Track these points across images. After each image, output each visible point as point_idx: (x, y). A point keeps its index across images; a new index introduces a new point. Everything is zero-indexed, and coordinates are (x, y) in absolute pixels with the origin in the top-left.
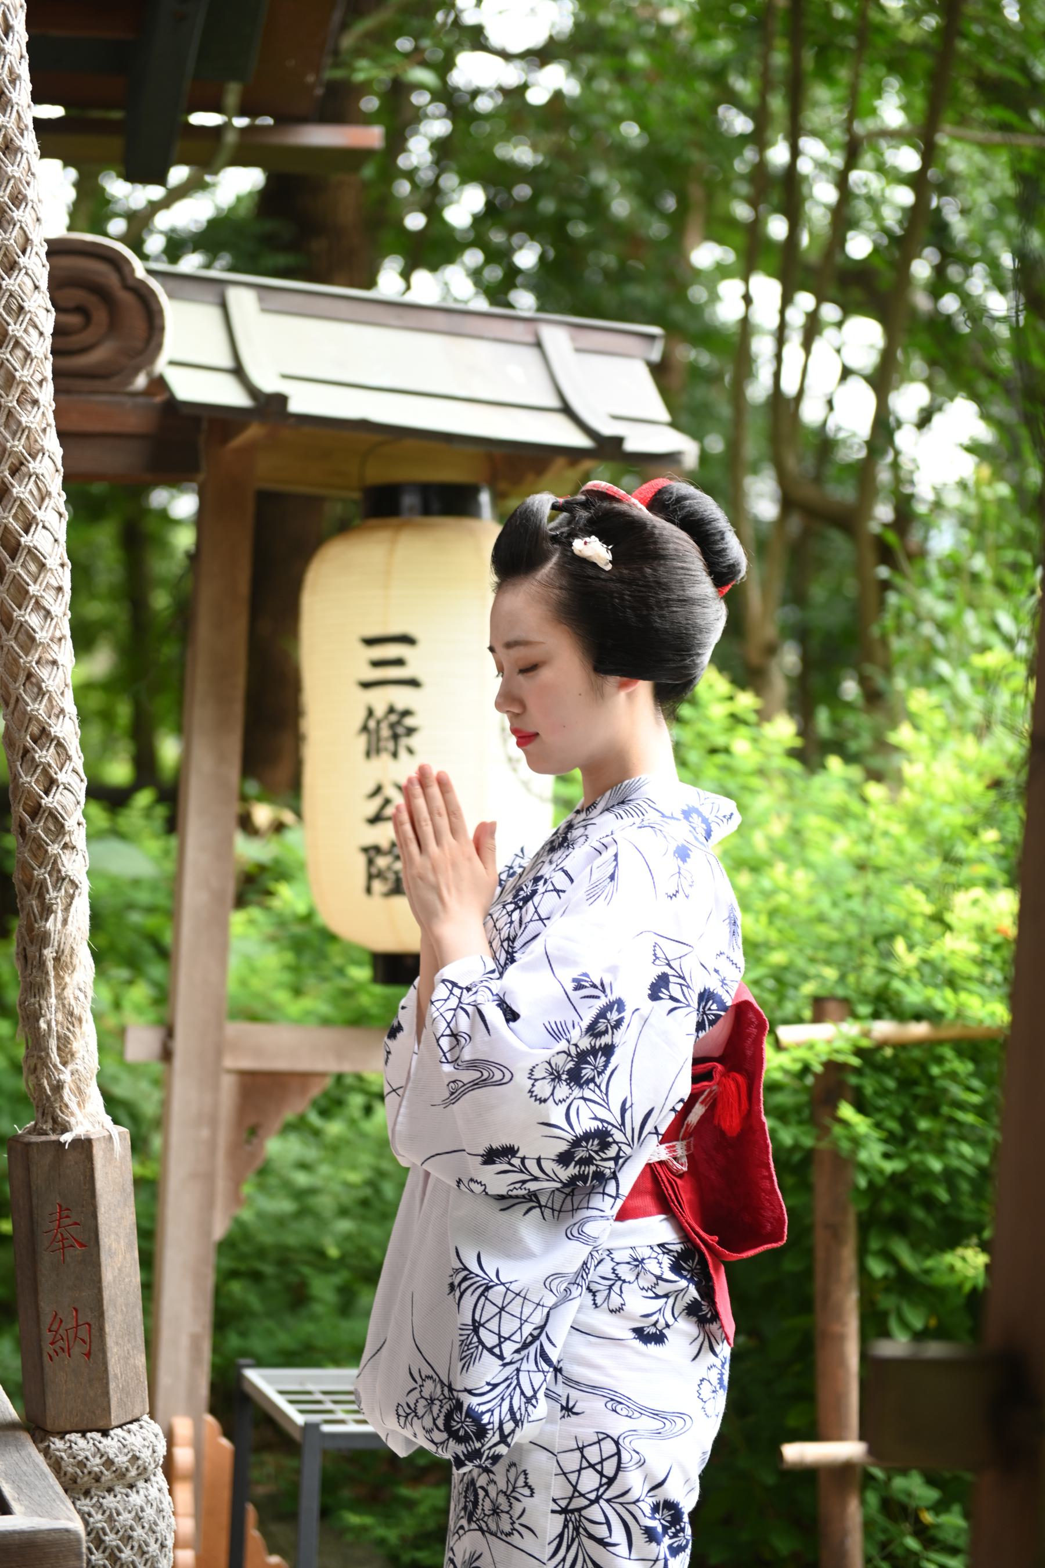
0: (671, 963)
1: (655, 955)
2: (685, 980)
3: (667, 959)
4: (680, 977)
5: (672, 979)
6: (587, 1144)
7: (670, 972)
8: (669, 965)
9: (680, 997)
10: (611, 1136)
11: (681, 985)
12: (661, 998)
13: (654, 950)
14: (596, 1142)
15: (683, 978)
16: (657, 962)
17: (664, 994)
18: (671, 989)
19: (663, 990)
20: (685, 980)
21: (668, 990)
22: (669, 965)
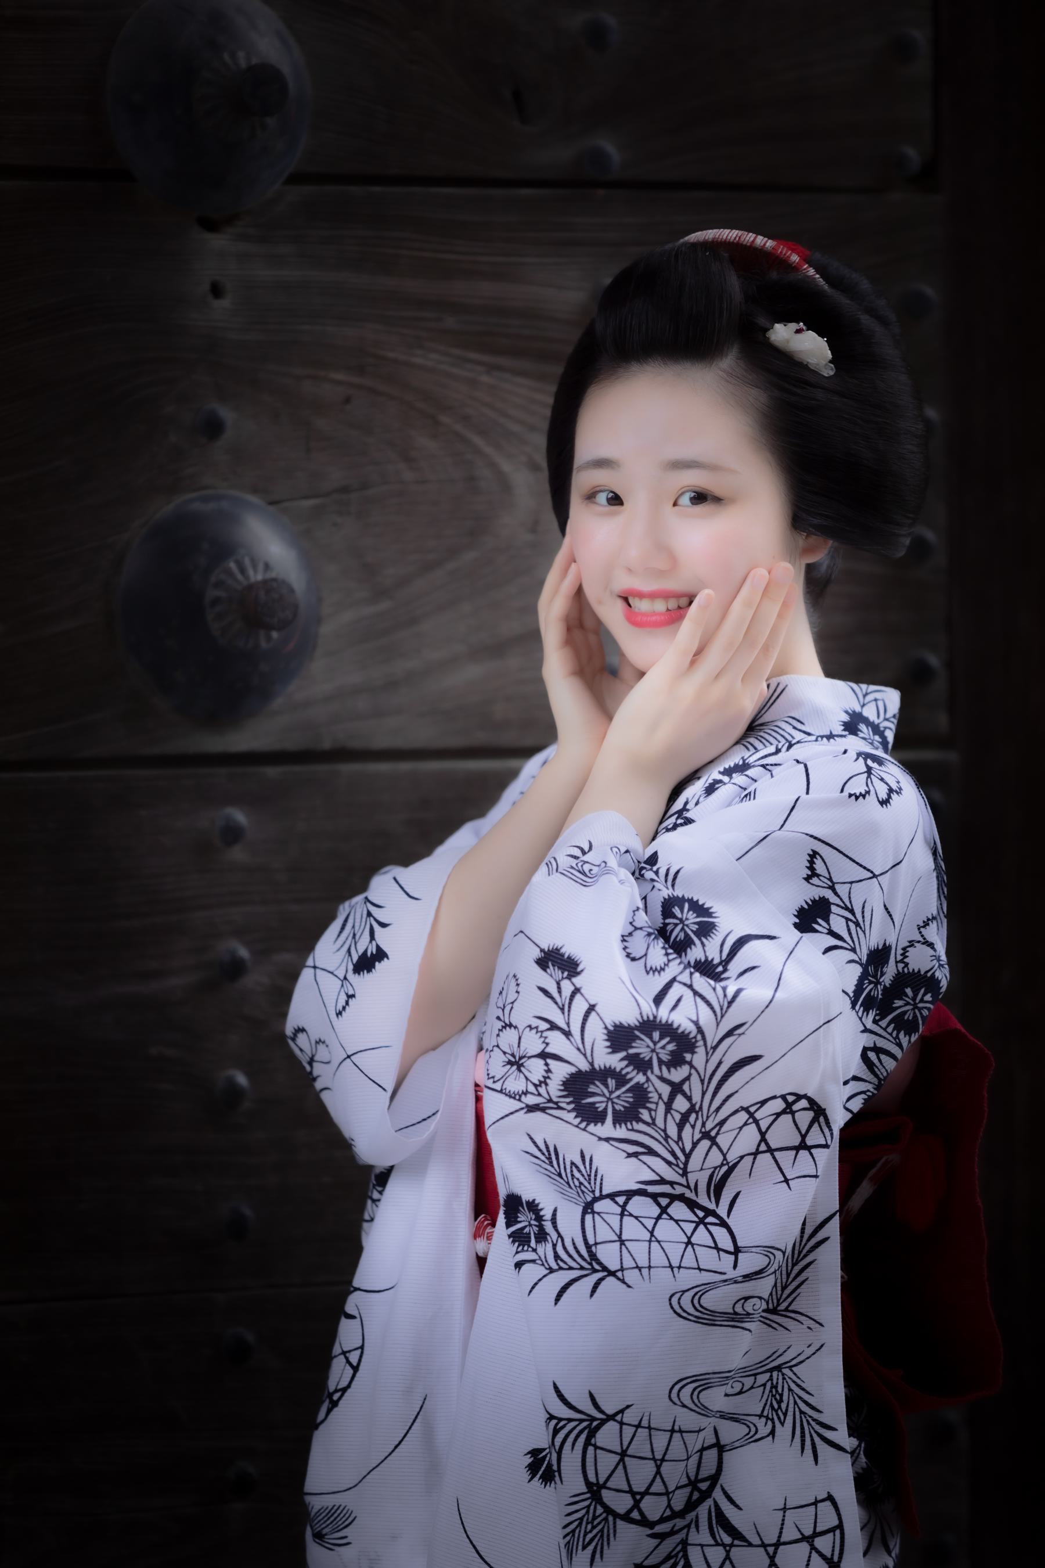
0: (837, 887)
1: (811, 868)
2: (852, 912)
3: (830, 879)
4: (846, 908)
5: (833, 908)
6: (661, 1038)
7: (833, 899)
8: (832, 888)
9: (845, 934)
10: (693, 1053)
11: (847, 919)
12: (816, 931)
13: (812, 862)
14: (671, 1047)
15: (852, 912)
16: (815, 881)
17: (821, 925)
18: (831, 922)
19: (820, 921)
20: (853, 914)
21: (828, 921)
22: (832, 888)
